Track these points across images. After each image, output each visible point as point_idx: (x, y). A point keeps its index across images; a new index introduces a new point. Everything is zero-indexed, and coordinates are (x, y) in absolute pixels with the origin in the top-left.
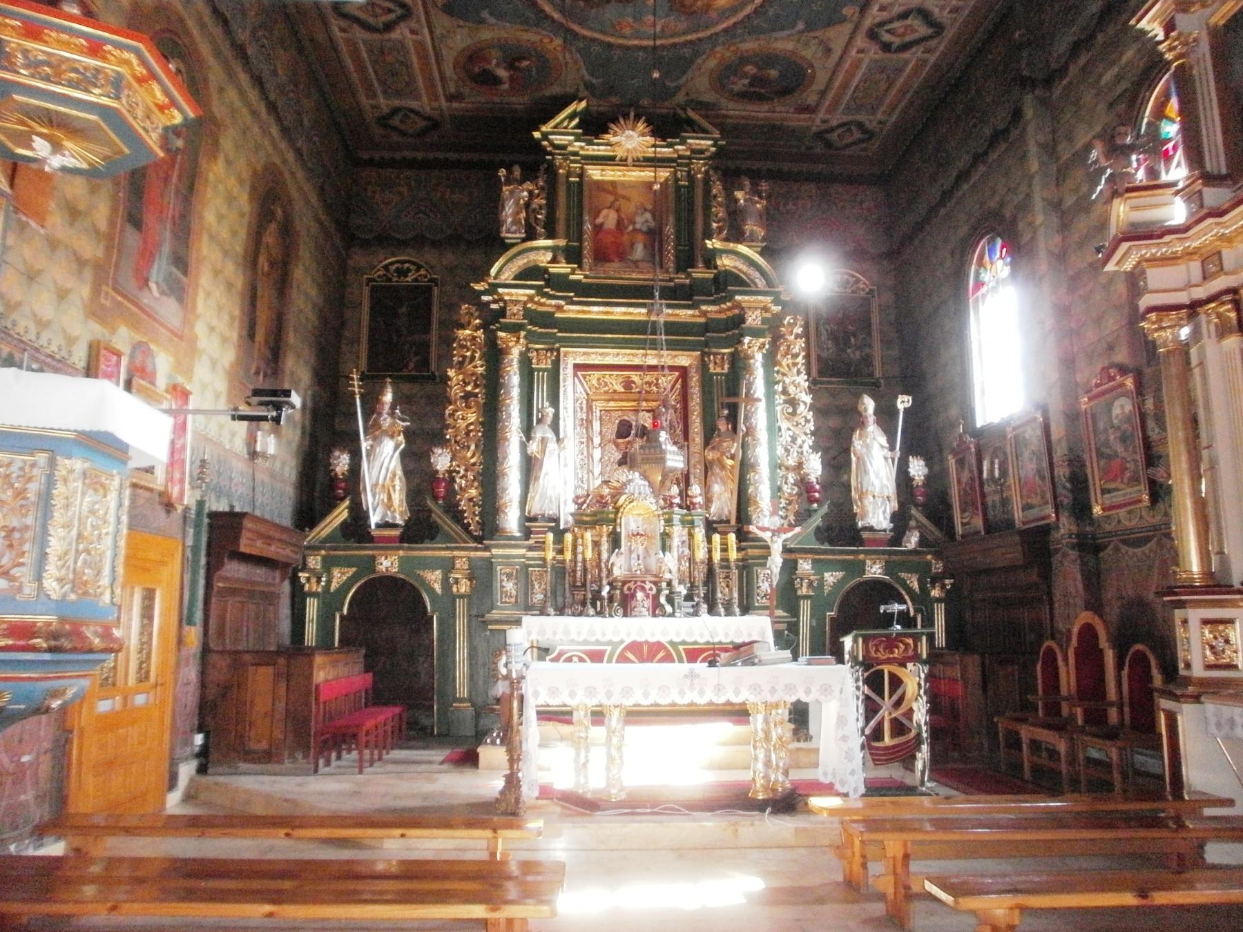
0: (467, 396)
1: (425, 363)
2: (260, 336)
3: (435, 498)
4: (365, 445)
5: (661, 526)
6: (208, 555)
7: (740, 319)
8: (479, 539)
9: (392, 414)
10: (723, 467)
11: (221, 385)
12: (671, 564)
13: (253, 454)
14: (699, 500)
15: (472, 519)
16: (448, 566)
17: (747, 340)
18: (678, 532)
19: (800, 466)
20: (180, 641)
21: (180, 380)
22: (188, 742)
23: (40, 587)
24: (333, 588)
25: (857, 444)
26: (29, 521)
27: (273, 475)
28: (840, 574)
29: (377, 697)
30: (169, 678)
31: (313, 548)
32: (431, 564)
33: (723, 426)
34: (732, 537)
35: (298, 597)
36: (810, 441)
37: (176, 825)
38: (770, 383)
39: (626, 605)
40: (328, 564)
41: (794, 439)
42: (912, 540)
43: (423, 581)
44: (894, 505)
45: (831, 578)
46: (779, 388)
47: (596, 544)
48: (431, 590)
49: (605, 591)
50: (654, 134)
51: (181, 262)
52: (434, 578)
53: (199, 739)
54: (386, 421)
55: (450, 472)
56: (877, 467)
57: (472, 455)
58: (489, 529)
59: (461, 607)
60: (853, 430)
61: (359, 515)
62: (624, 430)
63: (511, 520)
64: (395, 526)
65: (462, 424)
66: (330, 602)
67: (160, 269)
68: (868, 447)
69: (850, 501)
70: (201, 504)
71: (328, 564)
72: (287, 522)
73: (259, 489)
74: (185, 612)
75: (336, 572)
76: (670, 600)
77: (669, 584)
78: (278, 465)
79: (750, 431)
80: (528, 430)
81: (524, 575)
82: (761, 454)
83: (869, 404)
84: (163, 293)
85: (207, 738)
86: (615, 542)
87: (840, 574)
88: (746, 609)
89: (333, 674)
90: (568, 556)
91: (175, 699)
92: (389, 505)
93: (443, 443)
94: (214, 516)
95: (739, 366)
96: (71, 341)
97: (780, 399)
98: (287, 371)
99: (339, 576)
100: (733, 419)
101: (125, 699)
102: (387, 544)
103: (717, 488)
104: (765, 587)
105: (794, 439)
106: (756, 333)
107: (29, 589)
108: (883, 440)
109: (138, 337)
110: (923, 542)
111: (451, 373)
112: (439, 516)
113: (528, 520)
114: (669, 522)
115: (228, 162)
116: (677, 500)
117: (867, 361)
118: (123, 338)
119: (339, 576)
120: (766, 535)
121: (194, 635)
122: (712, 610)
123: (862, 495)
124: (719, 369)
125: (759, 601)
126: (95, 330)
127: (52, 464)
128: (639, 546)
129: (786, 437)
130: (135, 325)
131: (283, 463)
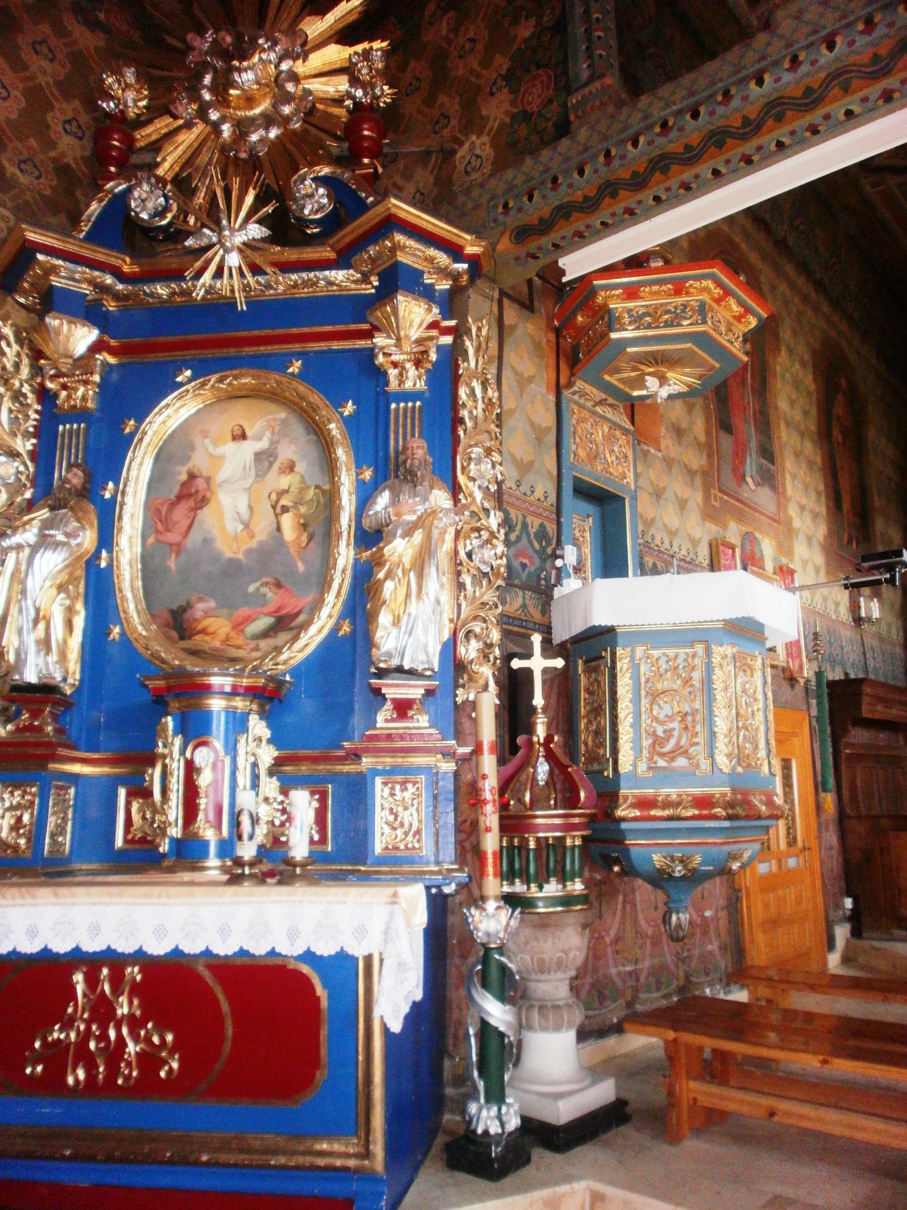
2: (846, 506)
6: (832, 723)
11: (819, 559)
13: (858, 621)
20: (819, 808)
21: (784, 561)
22: (839, 906)
23: (713, 763)
26: (697, 705)
27: (881, 639)
30: (814, 843)
37: (837, 984)
51: (767, 453)
67: (751, 465)
70: (819, 674)
73: (869, 655)
74: (819, 779)
78: (884, 626)
84: (757, 484)
85: (855, 903)
91: (822, 862)
94: (831, 684)
96: (695, 543)
98: (878, 534)
101: (779, 861)
107: (705, 765)
109: (744, 529)
115: (790, 351)
118: (733, 532)
121: (829, 800)
126: (712, 530)
127: (708, 652)
130: (740, 518)
131: (889, 626)
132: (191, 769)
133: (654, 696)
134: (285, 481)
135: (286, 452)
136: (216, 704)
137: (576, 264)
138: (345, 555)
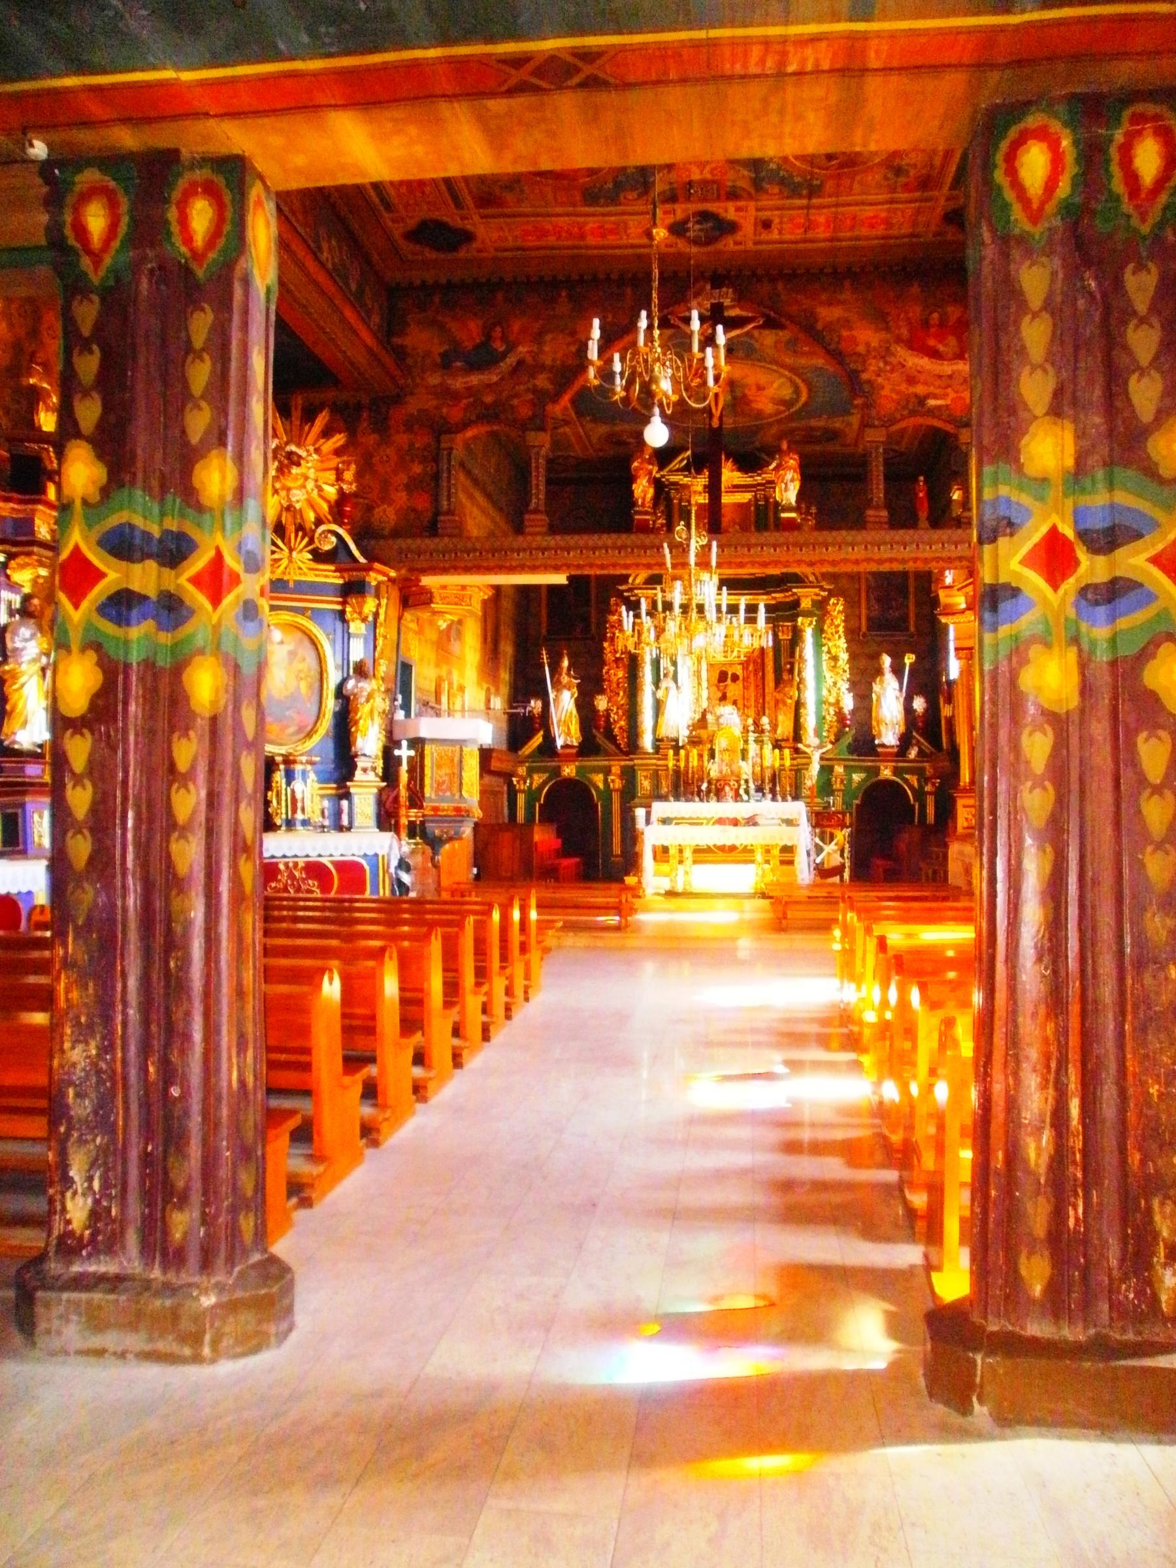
0: (617, 660)
1: (587, 629)
3: (598, 728)
4: (552, 695)
5: (741, 745)
7: (796, 603)
8: (627, 754)
9: (568, 674)
10: (785, 704)
12: (746, 769)
13: (488, 708)
14: (767, 727)
15: (622, 741)
16: (607, 771)
17: (800, 619)
18: (753, 748)
19: (838, 702)
24: (535, 786)
25: (876, 687)
28: (863, 775)
29: (565, 852)
31: (522, 763)
32: (597, 770)
33: (786, 676)
34: (787, 752)
35: (512, 794)
36: (847, 686)
38: (818, 646)
39: (719, 794)
40: (531, 772)
41: (835, 684)
42: (913, 753)
43: (590, 781)
44: (901, 728)
45: (857, 777)
46: (825, 649)
47: (701, 756)
48: (597, 788)
49: (704, 787)
50: (740, 469)
52: (599, 779)
53: (475, 871)
54: (565, 679)
55: (608, 711)
56: (890, 703)
57: (621, 699)
58: (633, 746)
59: (616, 798)
60: (874, 679)
61: (549, 739)
62: (723, 677)
63: (647, 742)
64: (572, 747)
65: (614, 679)
66: (532, 796)
68: (884, 689)
69: (870, 727)
71: (531, 772)
72: (504, 747)
75: (536, 777)
76: (747, 792)
77: (747, 781)
79: (801, 681)
80: (657, 683)
81: (656, 777)
82: (810, 697)
83: (886, 661)
86: (712, 755)
87: (863, 775)
88: (796, 797)
89: (542, 835)
90: (682, 764)
92: (568, 734)
93: (602, 691)
95: (797, 635)
97: (825, 657)
99: (538, 779)
100: (791, 671)
102: (568, 759)
103: (781, 718)
104: (809, 783)
105: (835, 684)
106: (807, 614)
108: (896, 685)
110: (921, 753)
111: (606, 645)
112: (600, 739)
113: (658, 741)
114: (746, 742)
116: (752, 728)
117: (905, 619)
119: (538, 779)
120: (807, 750)
122: (774, 799)
123: (878, 723)
124: (784, 636)
125: (805, 792)
128: (726, 757)
129: (830, 681)
132: (293, 792)
133: (439, 767)
134: (301, 666)
135: (300, 653)
136: (298, 768)
137: (427, 581)
138: (331, 704)
